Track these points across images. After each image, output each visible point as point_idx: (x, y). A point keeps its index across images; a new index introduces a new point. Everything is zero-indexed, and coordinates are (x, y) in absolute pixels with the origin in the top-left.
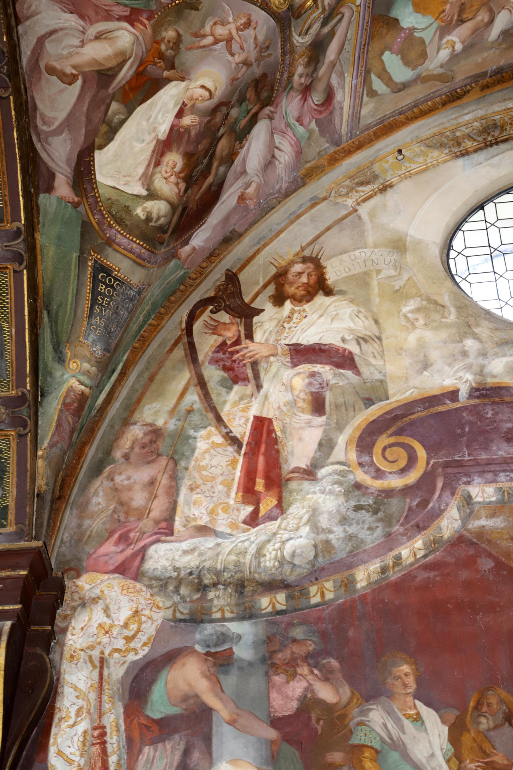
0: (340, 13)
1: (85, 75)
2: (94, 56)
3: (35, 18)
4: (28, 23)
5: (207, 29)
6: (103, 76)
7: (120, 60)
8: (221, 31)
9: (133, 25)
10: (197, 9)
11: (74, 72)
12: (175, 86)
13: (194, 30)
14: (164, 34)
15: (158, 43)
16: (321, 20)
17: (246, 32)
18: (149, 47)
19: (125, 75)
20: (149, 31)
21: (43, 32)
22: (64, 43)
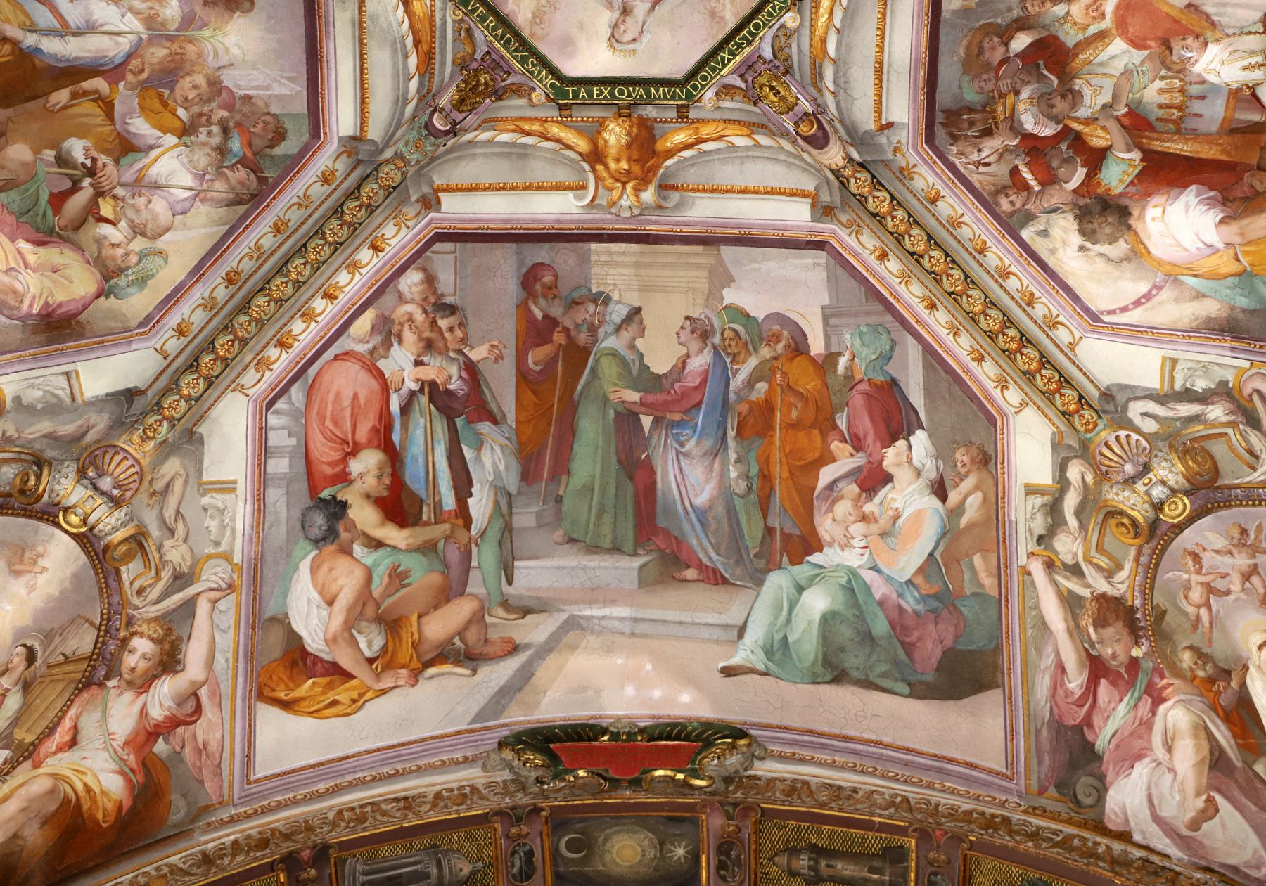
0: (1250, 395)
1: (1212, 786)
2: (1193, 762)
3: (1129, 813)
4: (1132, 824)
5: (1190, 610)
6: (1217, 762)
7: (1203, 735)
8: (1196, 594)
9: (1164, 700)
10: (1164, 612)
11: (1204, 797)
12: (1252, 680)
13: (1187, 626)
14: (1185, 665)
15: (1194, 677)
16: (1248, 429)
17: (1205, 563)
18: (1196, 691)
19: (1225, 737)
20: (1177, 682)
21: (1147, 812)
22: (1166, 792)
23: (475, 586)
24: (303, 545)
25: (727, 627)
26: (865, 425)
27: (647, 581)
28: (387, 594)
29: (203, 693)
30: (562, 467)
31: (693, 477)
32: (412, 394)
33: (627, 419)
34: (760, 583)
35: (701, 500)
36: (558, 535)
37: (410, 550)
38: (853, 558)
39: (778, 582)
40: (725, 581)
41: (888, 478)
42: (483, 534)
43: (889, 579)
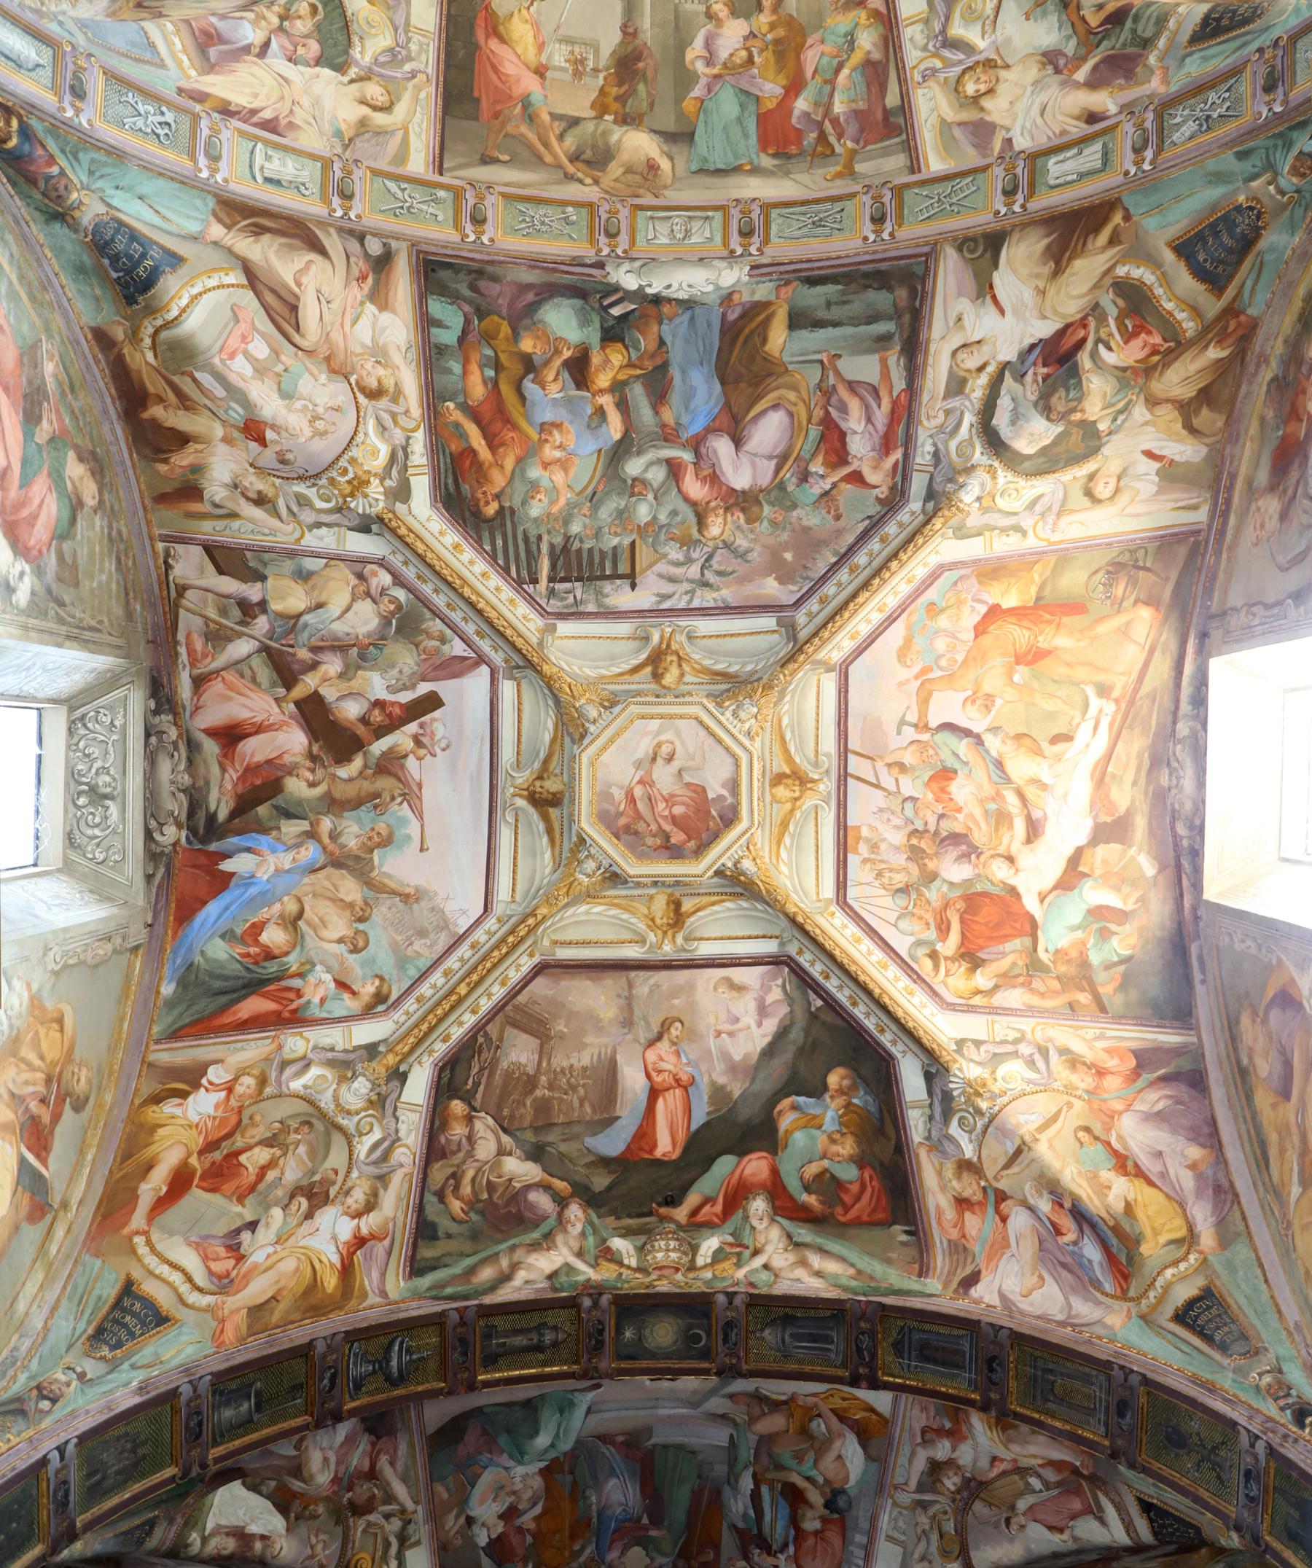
23: (753, 1440)
24: (853, 1493)
25: (598, 1411)
26: (515, 1540)
27: (648, 1431)
28: (805, 1451)
29: (919, 1440)
30: (696, 1496)
31: (618, 1493)
32: (781, 1552)
33: (656, 1521)
34: (577, 1442)
35: (613, 1482)
36: (701, 1457)
37: (790, 1470)
38: (520, 1470)
39: (566, 1445)
40: (599, 1438)
41: (501, 1517)
42: (746, 1467)
43: (498, 1465)
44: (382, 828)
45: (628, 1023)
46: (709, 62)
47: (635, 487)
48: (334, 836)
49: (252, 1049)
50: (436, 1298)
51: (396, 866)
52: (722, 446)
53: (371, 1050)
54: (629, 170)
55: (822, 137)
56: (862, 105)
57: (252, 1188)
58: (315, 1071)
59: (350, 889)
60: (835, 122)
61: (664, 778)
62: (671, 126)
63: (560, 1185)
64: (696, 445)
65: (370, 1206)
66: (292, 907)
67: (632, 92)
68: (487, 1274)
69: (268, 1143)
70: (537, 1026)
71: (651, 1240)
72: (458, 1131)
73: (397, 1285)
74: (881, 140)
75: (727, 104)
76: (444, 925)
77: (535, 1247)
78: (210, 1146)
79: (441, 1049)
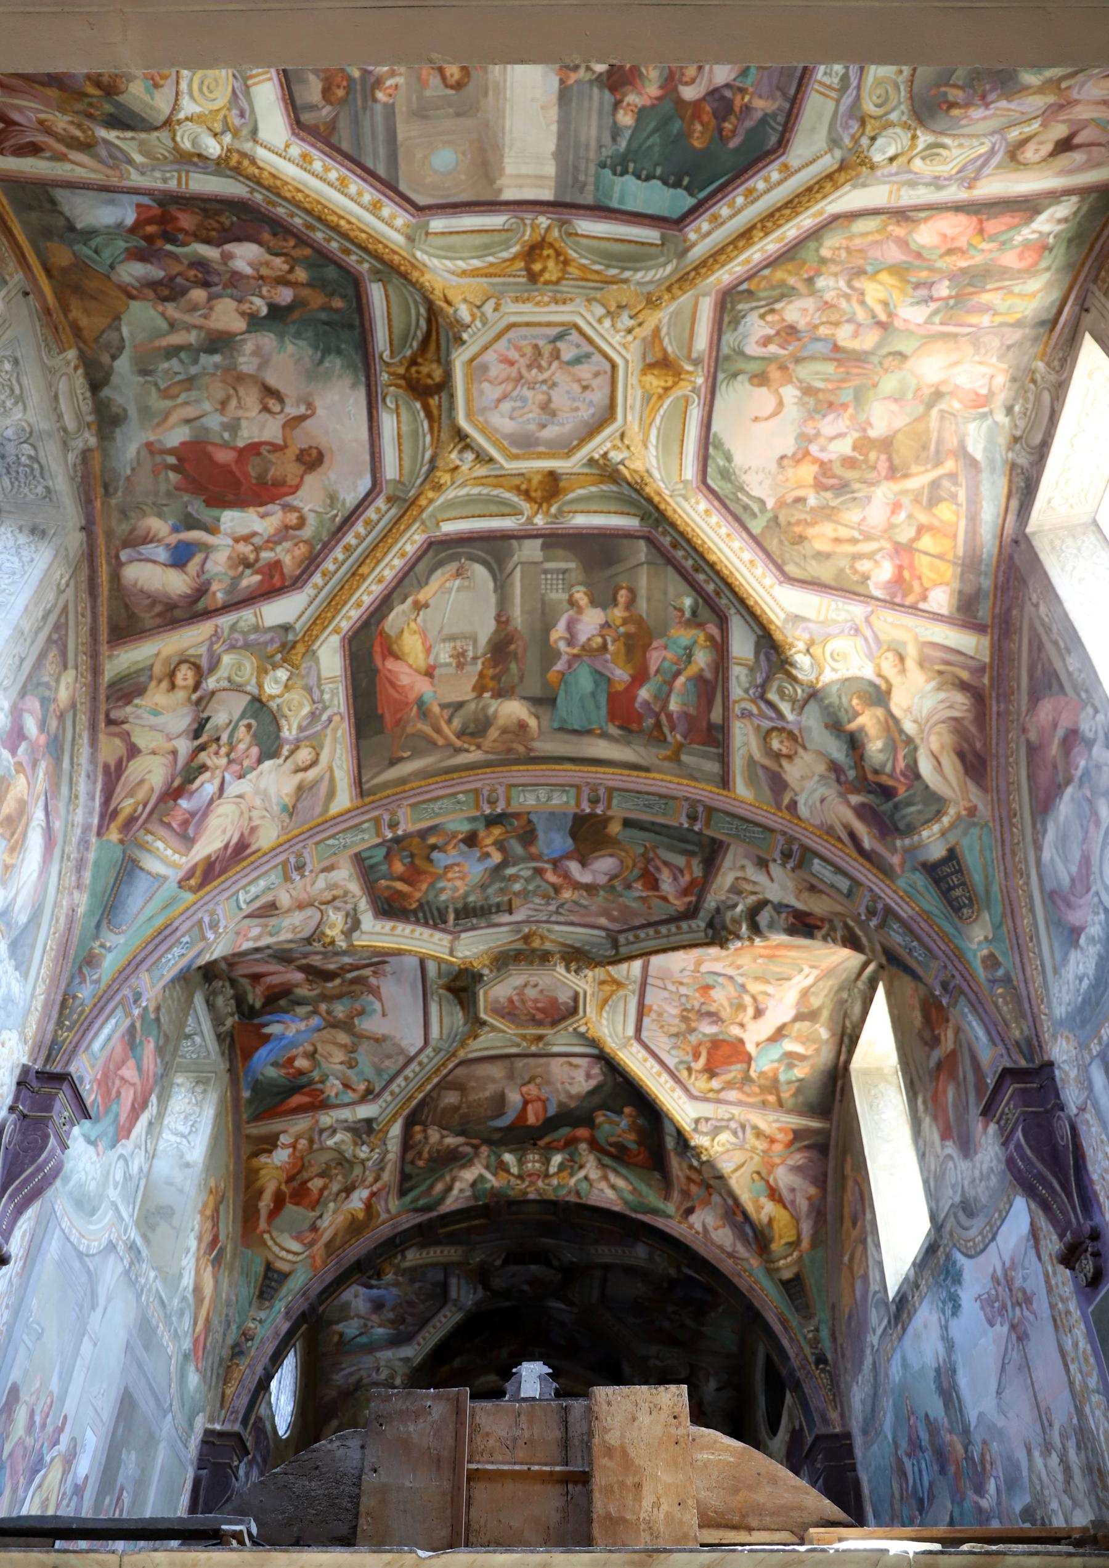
44: (357, 1006)
45: (511, 1076)
46: (571, 643)
47: (515, 878)
48: (329, 1012)
49: (301, 1124)
50: (416, 1210)
51: (370, 1025)
52: (574, 867)
53: (369, 1121)
54: (504, 731)
55: (658, 725)
56: (692, 711)
57: (318, 1202)
58: (338, 1137)
59: (343, 1038)
60: (669, 716)
61: (531, 993)
62: (537, 692)
63: (475, 1141)
64: (555, 863)
65: (376, 1180)
66: (310, 1048)
67: (506, 670)
68: (439, 1187)
69: (322, 1175)
70: (460, 1087)
71: (524, 1155)
72: (419, 1137)
73: (394, 1204)
74: (704, 744)
75: (584, 681)
76: (402, 1051)
77: (463, 1167)
78: (290, 1179)
79: (406, 1112)
